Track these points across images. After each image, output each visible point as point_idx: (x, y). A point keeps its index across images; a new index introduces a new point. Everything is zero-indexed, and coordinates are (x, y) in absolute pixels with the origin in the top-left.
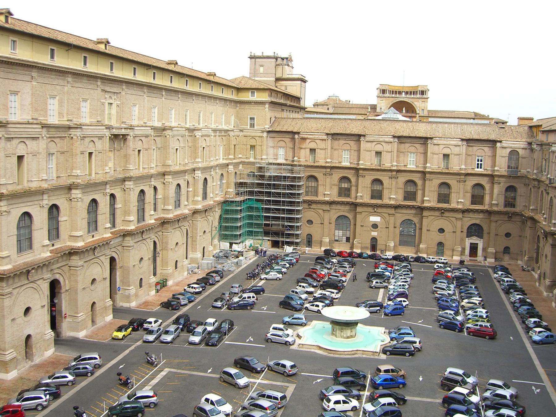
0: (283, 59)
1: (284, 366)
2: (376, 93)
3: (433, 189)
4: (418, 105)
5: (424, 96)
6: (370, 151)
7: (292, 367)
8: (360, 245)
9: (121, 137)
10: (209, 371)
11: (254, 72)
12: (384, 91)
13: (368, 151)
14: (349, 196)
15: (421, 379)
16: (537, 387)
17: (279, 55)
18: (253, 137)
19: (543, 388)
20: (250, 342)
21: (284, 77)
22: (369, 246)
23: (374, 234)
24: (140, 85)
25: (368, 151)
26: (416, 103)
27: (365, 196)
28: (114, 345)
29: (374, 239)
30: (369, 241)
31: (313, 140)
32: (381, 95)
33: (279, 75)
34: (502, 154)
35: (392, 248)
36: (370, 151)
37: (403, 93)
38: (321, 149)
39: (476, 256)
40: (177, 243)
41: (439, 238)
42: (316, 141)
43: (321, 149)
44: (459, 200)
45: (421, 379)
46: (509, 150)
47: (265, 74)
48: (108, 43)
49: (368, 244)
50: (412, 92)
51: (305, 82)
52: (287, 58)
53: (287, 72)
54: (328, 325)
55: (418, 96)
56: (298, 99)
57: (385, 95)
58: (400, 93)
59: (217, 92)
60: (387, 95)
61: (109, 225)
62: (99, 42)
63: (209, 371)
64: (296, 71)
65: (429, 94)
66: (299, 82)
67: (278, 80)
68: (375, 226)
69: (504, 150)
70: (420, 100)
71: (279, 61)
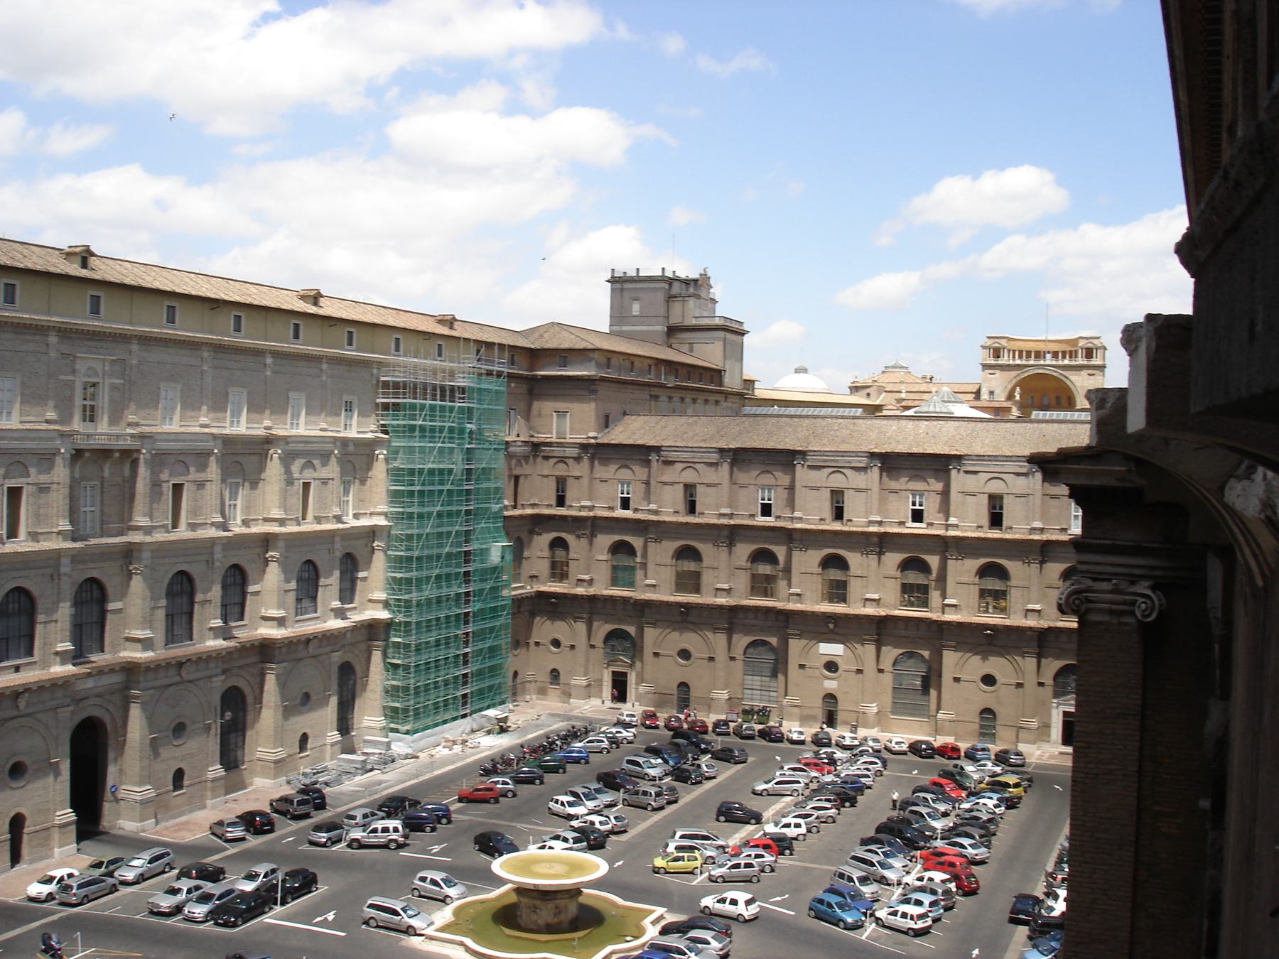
0: (687, 282)
3: (964, 579)
5: (1096, 361)
6: (817, 489)
8: (796, 710)
9: (117, 455)
11: (619, 314)
13: (813, 488)
14: (925, 603)
17: (682, 274)
18: (562, 460)
20: (324, 924)
21: (686, 323)
22: (820, 714)
23: (831, 685)
25: (813, 488)
26: (1072, 378)
27: (808, 594)
29: (830, 697)
31: (690, 465)
33: (675, 320)
35: (872, 718)
36: (817, 489)
37: (1048, 356)
38: (709, 485)
40: (307, 696)
41: (985, 697)
42: (697, 466)
43: (709, 485)
44: (1030, 606)
47: (642, 318)
49: (817, 707)
51: (742, 333)
52: (696, 281)
53: (690, 313)
56: (716, 375)
58: (1038, 355)
60: (1005, 360)
62: (69, 255)
64: (726, 309)
66: (721, 334)
67: (672, 331)
68: (831, 666)
70: (1084, 373)
71: (676, 288)
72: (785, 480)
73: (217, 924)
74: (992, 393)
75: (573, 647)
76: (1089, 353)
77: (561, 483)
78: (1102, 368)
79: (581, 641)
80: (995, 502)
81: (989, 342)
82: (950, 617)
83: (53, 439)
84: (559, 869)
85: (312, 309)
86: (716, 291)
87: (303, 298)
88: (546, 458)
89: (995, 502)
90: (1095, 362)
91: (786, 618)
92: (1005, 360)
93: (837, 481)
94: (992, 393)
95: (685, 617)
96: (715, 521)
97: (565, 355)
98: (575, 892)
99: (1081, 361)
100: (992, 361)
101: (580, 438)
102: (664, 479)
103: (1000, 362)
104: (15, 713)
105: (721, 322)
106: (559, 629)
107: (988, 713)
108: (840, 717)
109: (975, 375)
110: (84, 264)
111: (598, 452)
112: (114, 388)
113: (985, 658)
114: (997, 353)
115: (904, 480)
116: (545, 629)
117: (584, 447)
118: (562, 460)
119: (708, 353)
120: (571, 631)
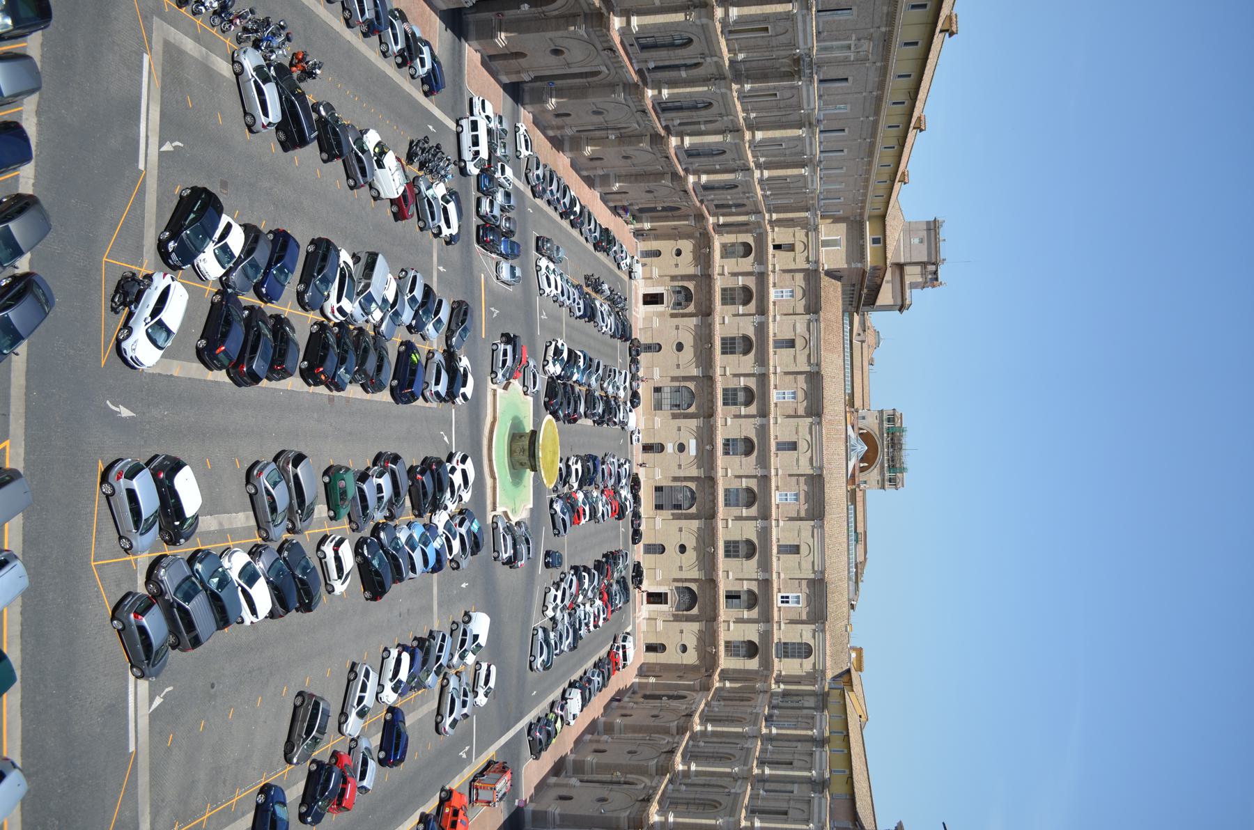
0: (935, 273)
1: (464, 385)
2: (888, 408)
4: (874, 475)
5: (887, 483)
7: (464, 396)
10: (441, 268)
11: (909, 229)
12: (891, 419)
15: (464, 585)
16: (469, 753)
19: (469, 760)
20: (490, 313)
23: (670, 448)
24: (881, 86)
28: (462, 102)
29: (661, 448)
30: (657, 441)
32: (885, 417)
34: (805, 634)
39: (649, 602)
45: (464, 585)
46: (811, 643)
48: (951, 35)
50: (895, 465)
52: (937, 279)
54: (529, 427)
55: (887, 475)
56: (871, 301)
57: (885, 423)
59: (876, 187)
60: (886, 425)
61: (651, 65)
63: (441, 268)
65: (890, 491)
67: (900, 267)
68: (682, 448)
69: (810, 635)
70: (879, 478)
71: (931, 268)
72: (801, 411)
73: (478, 227)
74: (864, 418)
75: (677, 265)
76: (892, 481)
77: (791, 248)
78: (883, 487)
79: (683, 271)
80: (795, 549)
81: (898, 414)
82: (720, 524)
83: (805, 43)
84: (549, 458)
85: (912, 125)
86: (929, 290)
87: (919, 118)
88: (807, 235)
89: (795, 549)
90: (887, 483)
91: (709, 414)
92: (886, 425)
93: (802, 446)
94: (864, 418)
95: (704, 338)
96: (771, 363)
97: (880, 241)
98: (534, 468)
99: (887, 475)
100: (885, 417)
101: (823, 259)
102: (798, 325)
103: (885, 423)
104: (600, 47)
105: (908, 302)
106: (688, 255)
107: (662, 549)
108: (650, 456)
109: (876, 405)
110: (942, 31)
111: (812, 276)
112: (847, 57)
113: (695, 549)
114: (891, 419)
115: (806, 488)
116: (687, 246)
117: (817, 262)
118: (806, 247)
119: (886, 295)
120: (687, 265)
